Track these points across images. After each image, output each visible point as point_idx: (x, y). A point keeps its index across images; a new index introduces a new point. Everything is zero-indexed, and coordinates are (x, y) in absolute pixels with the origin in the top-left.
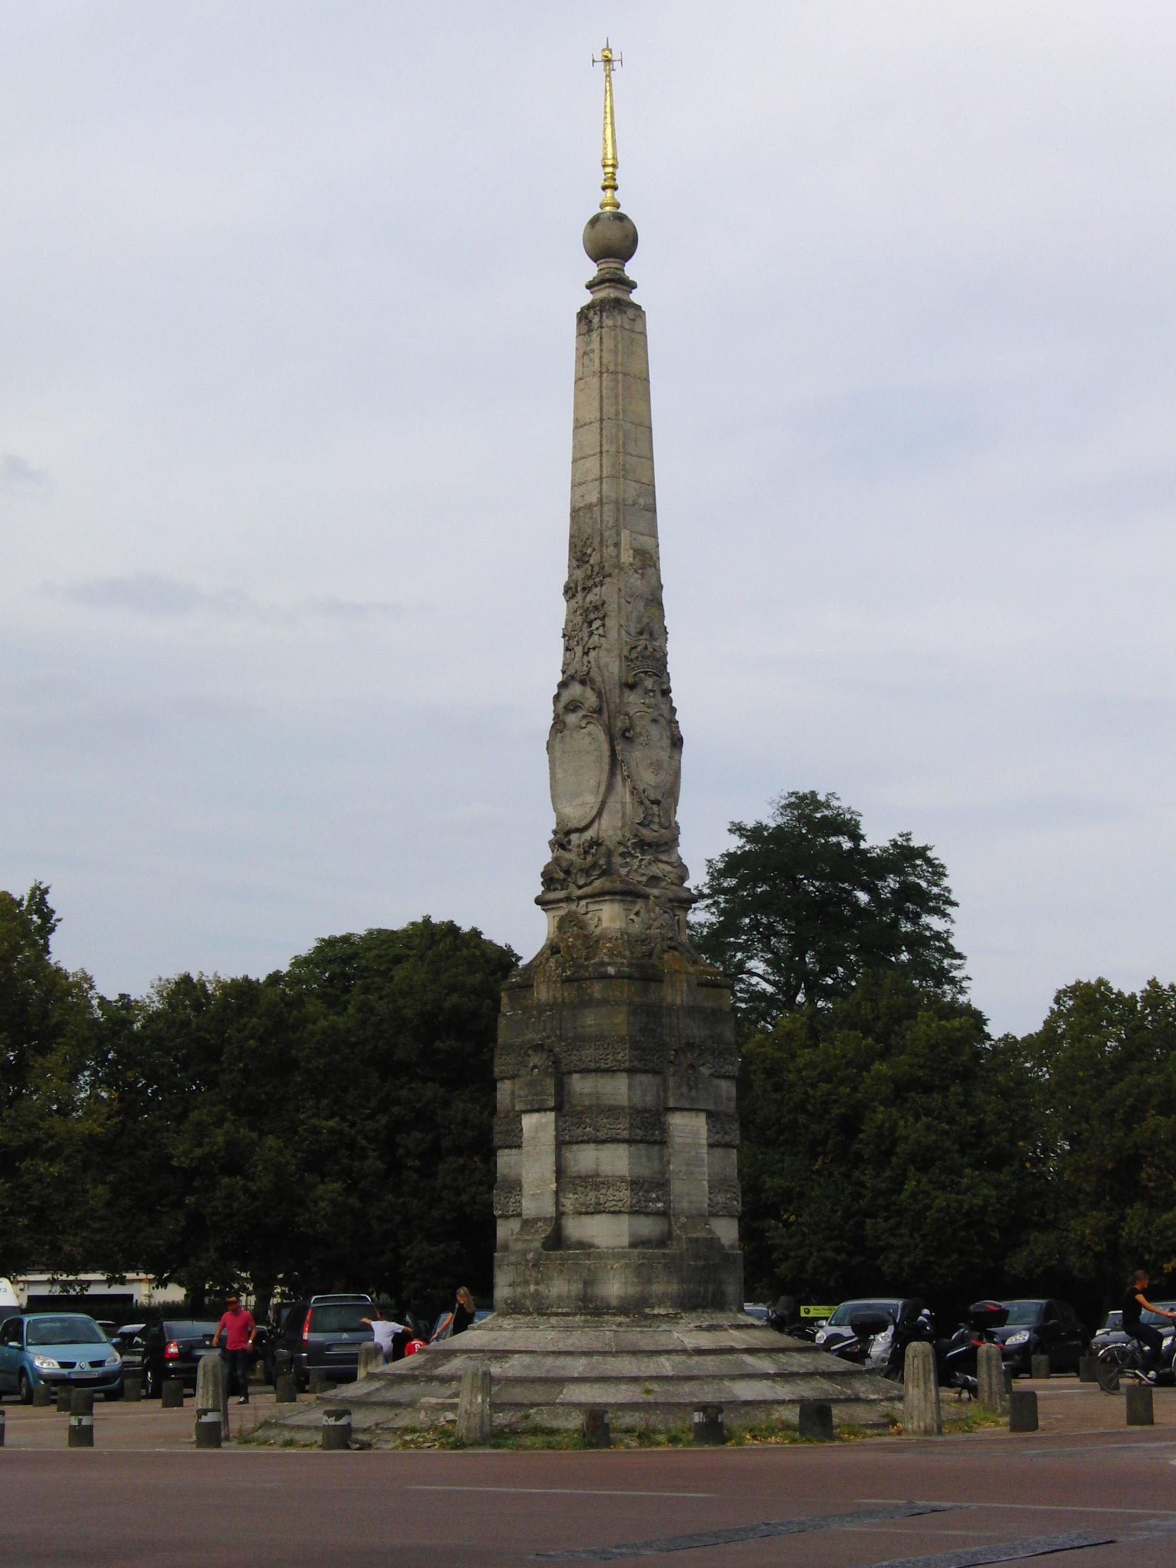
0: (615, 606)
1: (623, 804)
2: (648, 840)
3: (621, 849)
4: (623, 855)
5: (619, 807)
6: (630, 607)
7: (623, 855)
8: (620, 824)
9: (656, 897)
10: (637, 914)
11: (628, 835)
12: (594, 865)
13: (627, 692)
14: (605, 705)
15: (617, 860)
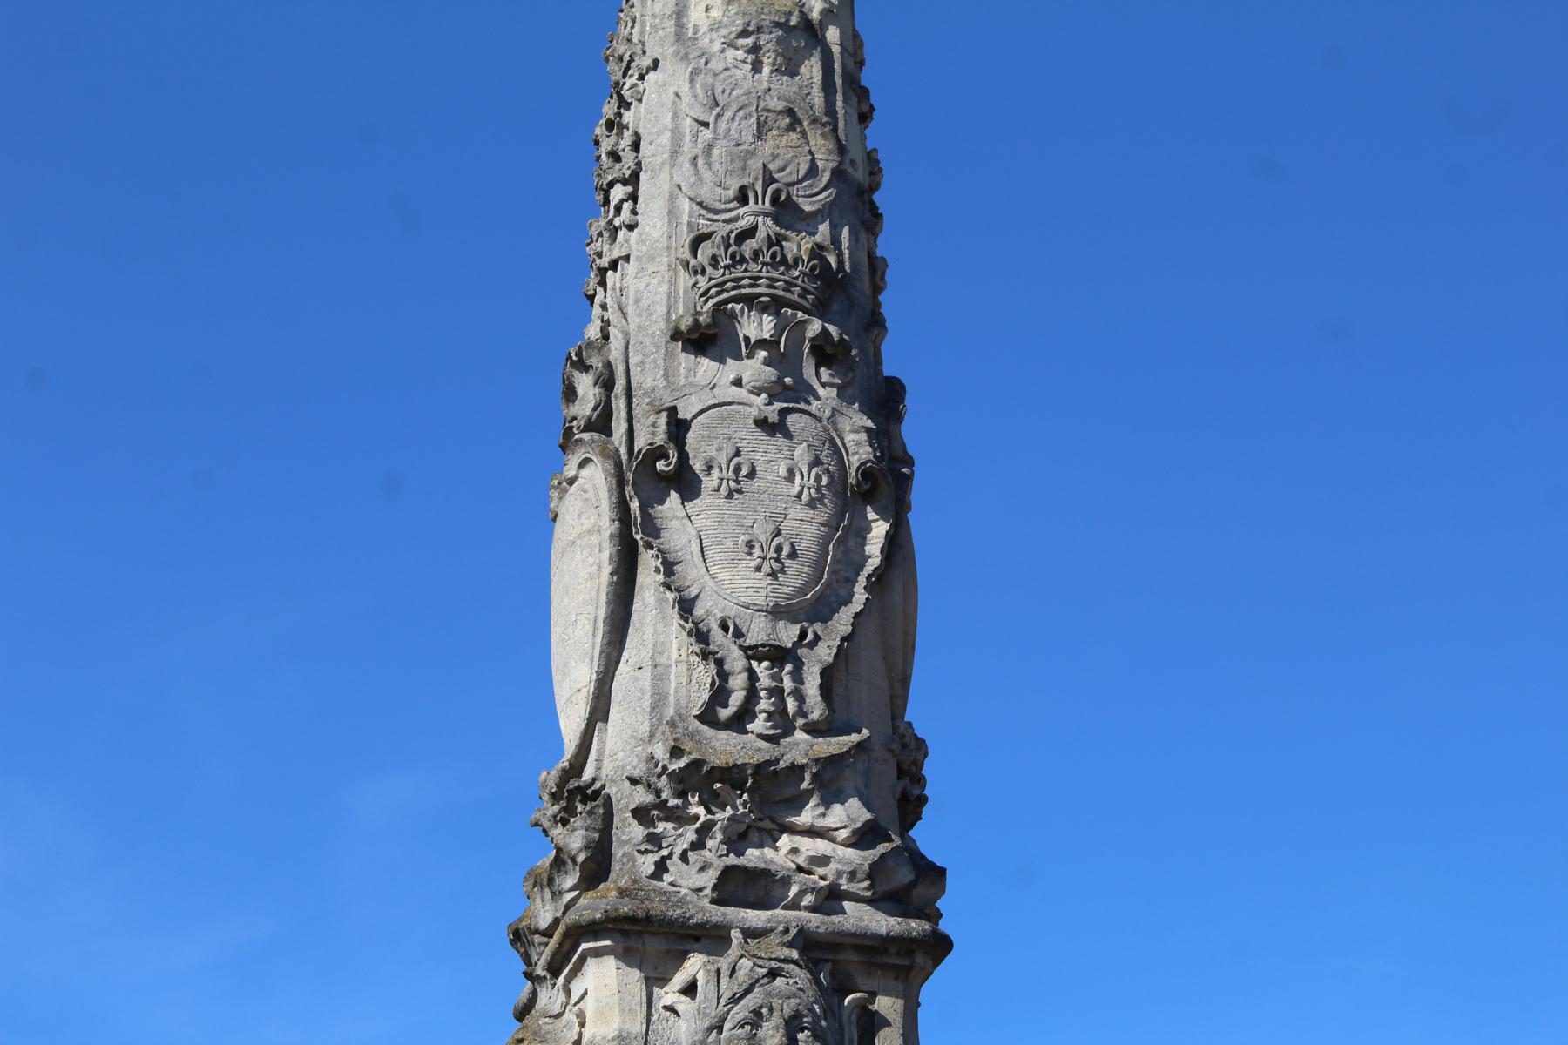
0: (666, 139)
1: (659, 673)
2: (717, 761)
3: (642, 797)
4: (641, 814)
5: (646, 675)
6: (707, 134)
7: (641, 814)
8: (645, 728)
9: (750, 933)
10: (690, 990)
11: (661, 752)
12: (559, 863)
13: (685, 360)
14: (619, 405)
15: (629, 832)
